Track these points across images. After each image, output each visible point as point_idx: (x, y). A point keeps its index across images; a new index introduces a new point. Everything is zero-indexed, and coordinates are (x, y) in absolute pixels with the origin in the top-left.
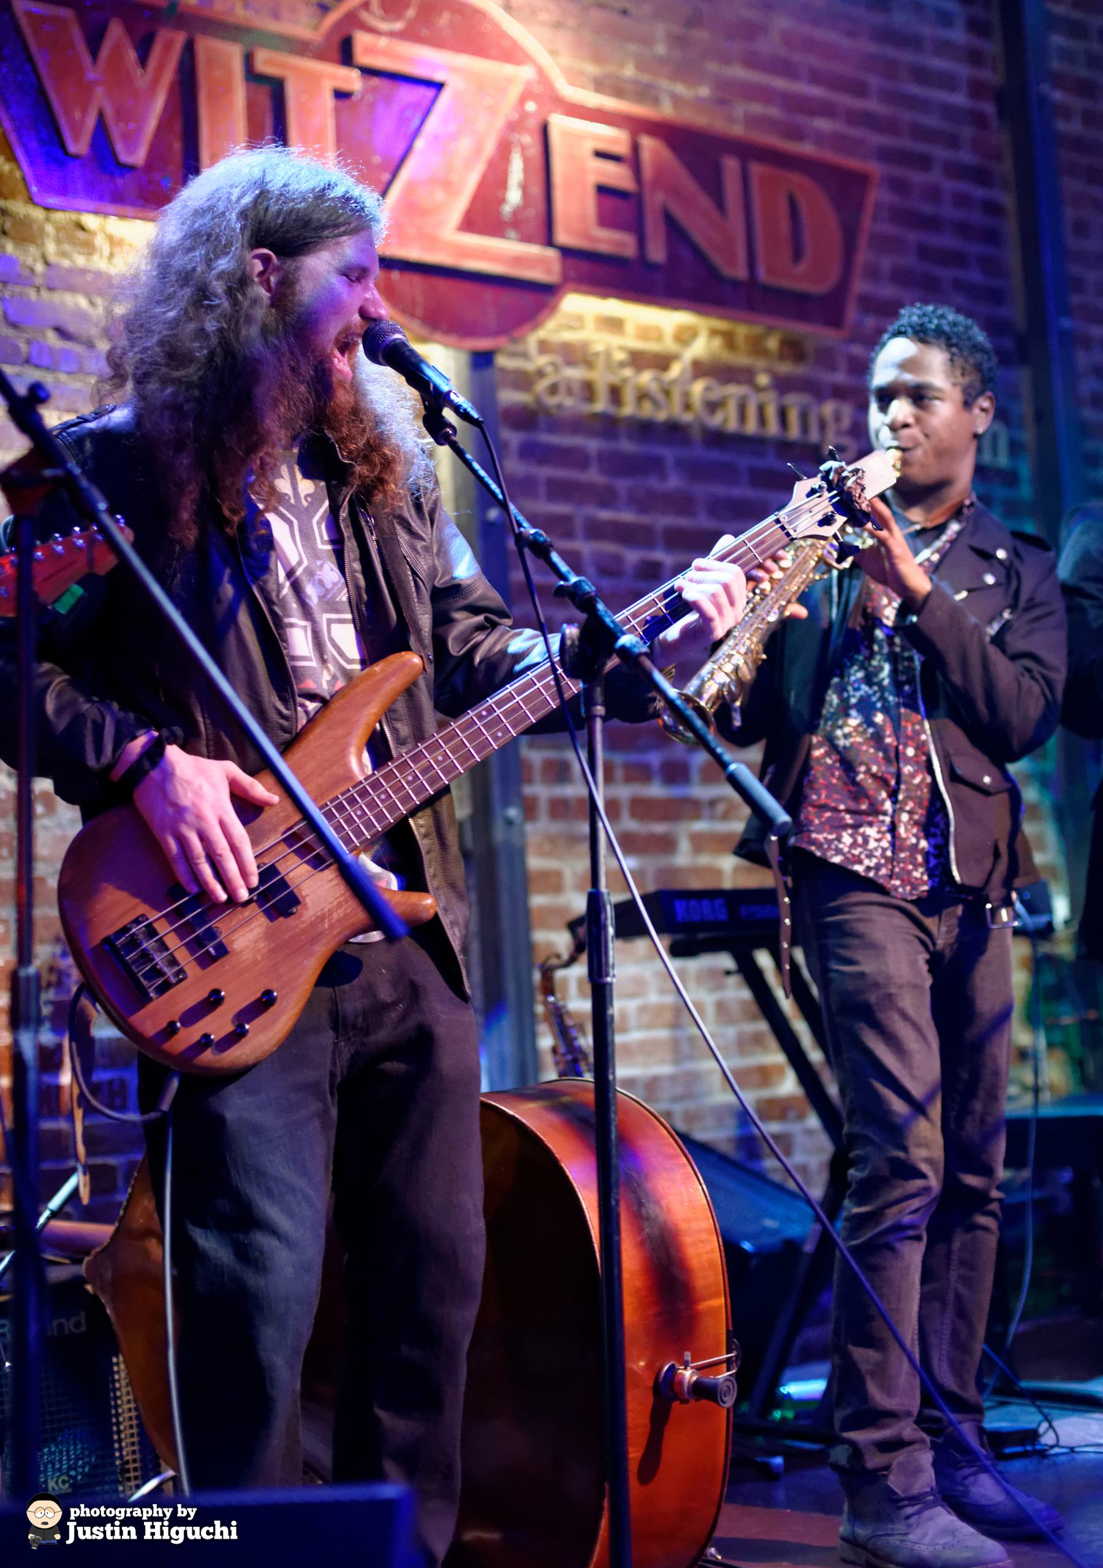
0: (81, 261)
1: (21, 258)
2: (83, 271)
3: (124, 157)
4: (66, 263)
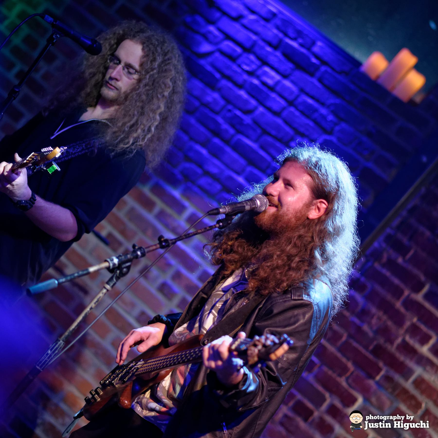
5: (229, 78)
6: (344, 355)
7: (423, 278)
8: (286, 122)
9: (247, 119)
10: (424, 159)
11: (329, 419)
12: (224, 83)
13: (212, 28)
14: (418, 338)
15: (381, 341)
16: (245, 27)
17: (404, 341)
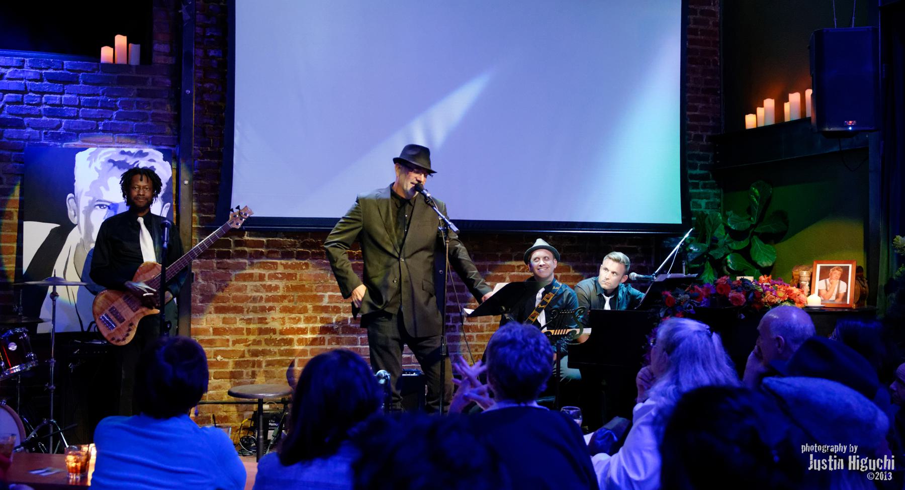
5: (29, 115)
8: (85, 119)
9: (61, 131)
10: (188, 92)
11: (239, 248)
12: (26, 119)
16: (8, 79)
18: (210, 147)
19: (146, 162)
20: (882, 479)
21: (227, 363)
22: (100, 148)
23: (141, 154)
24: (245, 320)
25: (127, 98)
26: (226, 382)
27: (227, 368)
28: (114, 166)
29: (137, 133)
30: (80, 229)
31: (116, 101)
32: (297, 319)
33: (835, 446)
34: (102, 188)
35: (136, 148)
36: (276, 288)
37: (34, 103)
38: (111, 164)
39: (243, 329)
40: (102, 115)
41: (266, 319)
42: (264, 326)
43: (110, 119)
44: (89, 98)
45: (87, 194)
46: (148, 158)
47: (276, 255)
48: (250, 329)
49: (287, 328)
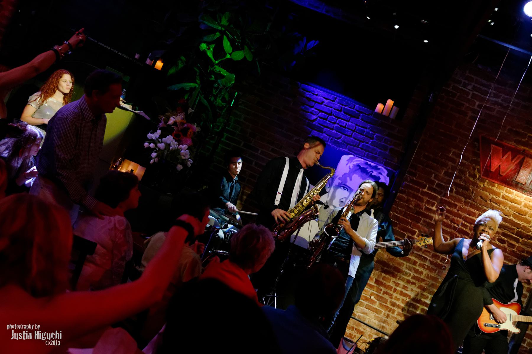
0: (490, 187)
1: (479, 184)
2: (491, 189)
3: (501, 173)
4: (488, 187)
5: (327, 127)
6: (407, 218)
7: (425, 183)
8: (354, 138)
10: (416, 142)
13: (313, 109)
14: (430, 204)
15: (418, 209)
16: (325, 105)
17: (426, 207)
18: (415, 177)
19: (377, 173)
20: (54, 345)
21: (376, 302)
22: (356, 157)
23: (376, 168)
24: (395, 283)
25: (381, 135)
26: (371, 313)
27: (375, 305)
28: (359, 169)
29: (378, 155)
30: (328, 195)
31: (374, 135)
32: (426, 296)
33: (27, 325)
34: (348, 178)
35: (375, 163)
36: (421, 273)
37: (332, 121)
38: (358, 168)
39: (392, 287)
40: (364, 140)
41: (407, 288)
42: (404, 291)
43: (367, 143)
44: (361, 128)
45: (339, 179)
46: (379, 171)
47: (428, 254)
48: (396, 289)
49: (418, 299)
